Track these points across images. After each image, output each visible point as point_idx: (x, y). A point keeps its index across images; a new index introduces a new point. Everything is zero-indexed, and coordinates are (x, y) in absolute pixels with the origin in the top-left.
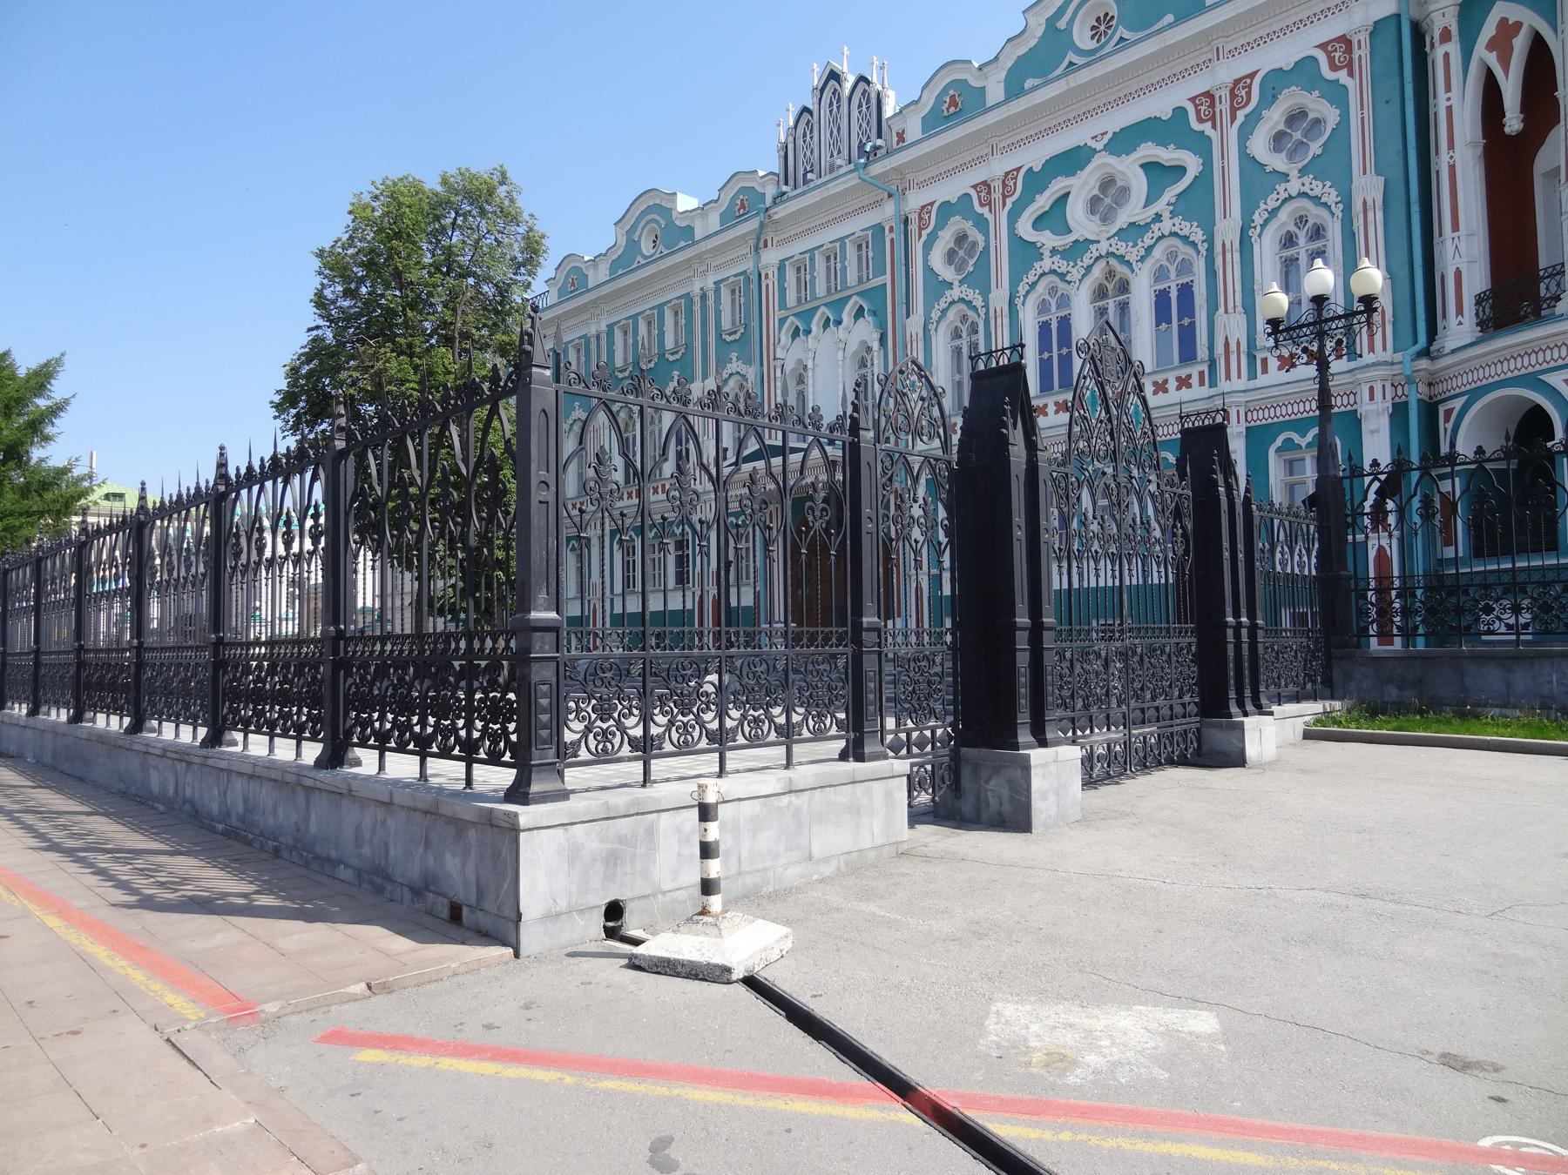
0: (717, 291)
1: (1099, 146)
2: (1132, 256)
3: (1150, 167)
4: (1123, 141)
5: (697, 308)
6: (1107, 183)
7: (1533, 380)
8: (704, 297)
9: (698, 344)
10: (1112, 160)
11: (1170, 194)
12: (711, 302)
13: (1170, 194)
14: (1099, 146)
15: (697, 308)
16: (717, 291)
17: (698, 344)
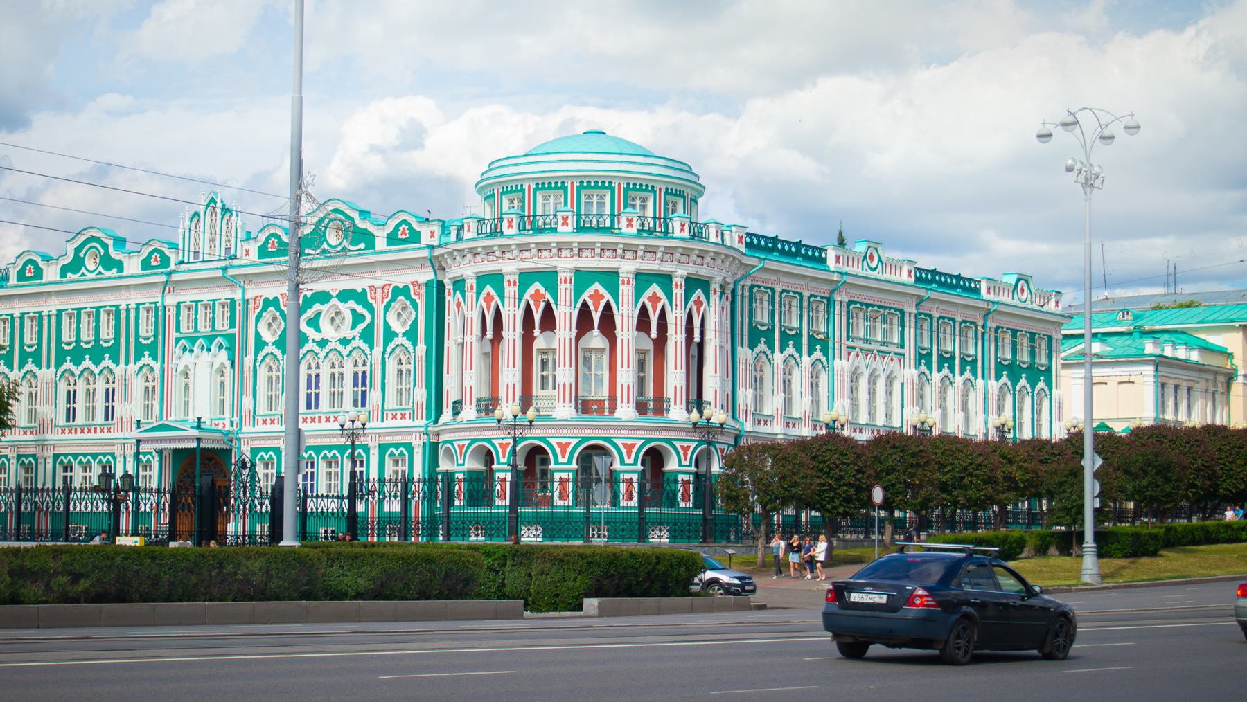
0: (137, 309)
1: (334, 294)
2: (345, 352)
3: (353, 311)
4: (345, 296)
5: (123, 315)
6: (338, 313)
7: (489, 440)
8: (128, 310)
9: (123, 340)
10: (339, 303)
11: (361, 326)
12: (133, 315)
13: (361, 326)
14: (334, 294)
15: (123, 315)
16: (137, 309)
17: (123, 340)
